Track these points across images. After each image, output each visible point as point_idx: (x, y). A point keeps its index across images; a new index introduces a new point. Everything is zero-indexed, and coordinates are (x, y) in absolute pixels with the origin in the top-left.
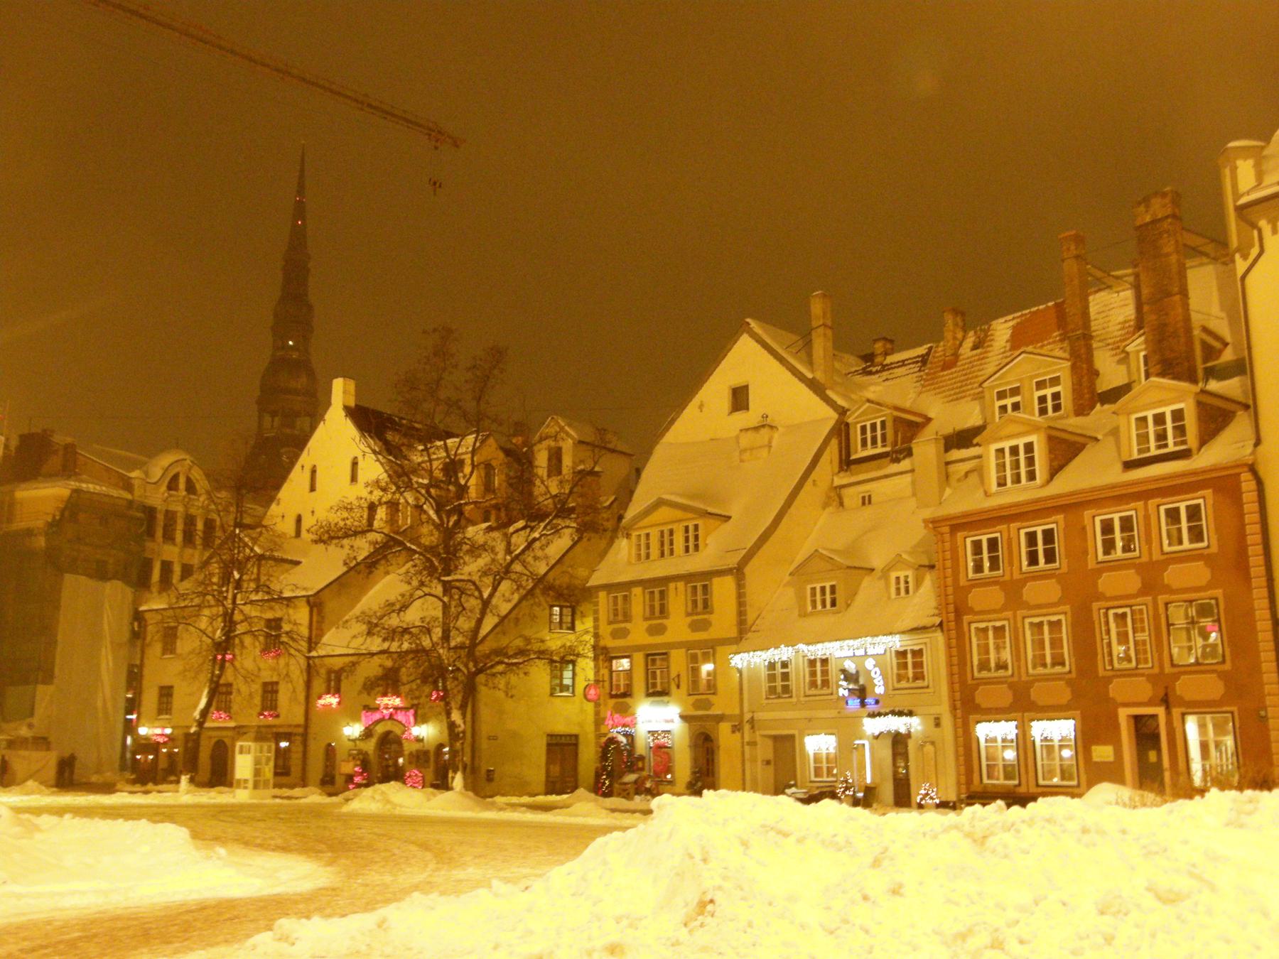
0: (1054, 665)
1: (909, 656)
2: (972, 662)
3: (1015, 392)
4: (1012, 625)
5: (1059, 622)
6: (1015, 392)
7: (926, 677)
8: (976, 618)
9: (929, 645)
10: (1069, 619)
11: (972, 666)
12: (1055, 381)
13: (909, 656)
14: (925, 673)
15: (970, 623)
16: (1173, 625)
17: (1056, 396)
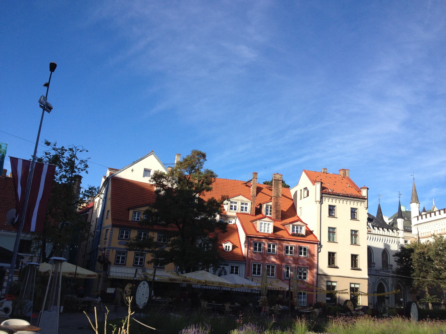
0: (257, 274)
1: (235, 268)
2: (252, 272)
3: (236, 203)
4: (263, 264)
5: (274, 266)
6: (236, 203)
7: (239, 274)
8: (254, 261)
9: (241, 266)
10: (277, 267)
11: (252, 273)
12: (246, 204)
13: (235, 268)
14: (239, 273)
15: (252, 263)
16: (299, 271)
17: (246, 208)
